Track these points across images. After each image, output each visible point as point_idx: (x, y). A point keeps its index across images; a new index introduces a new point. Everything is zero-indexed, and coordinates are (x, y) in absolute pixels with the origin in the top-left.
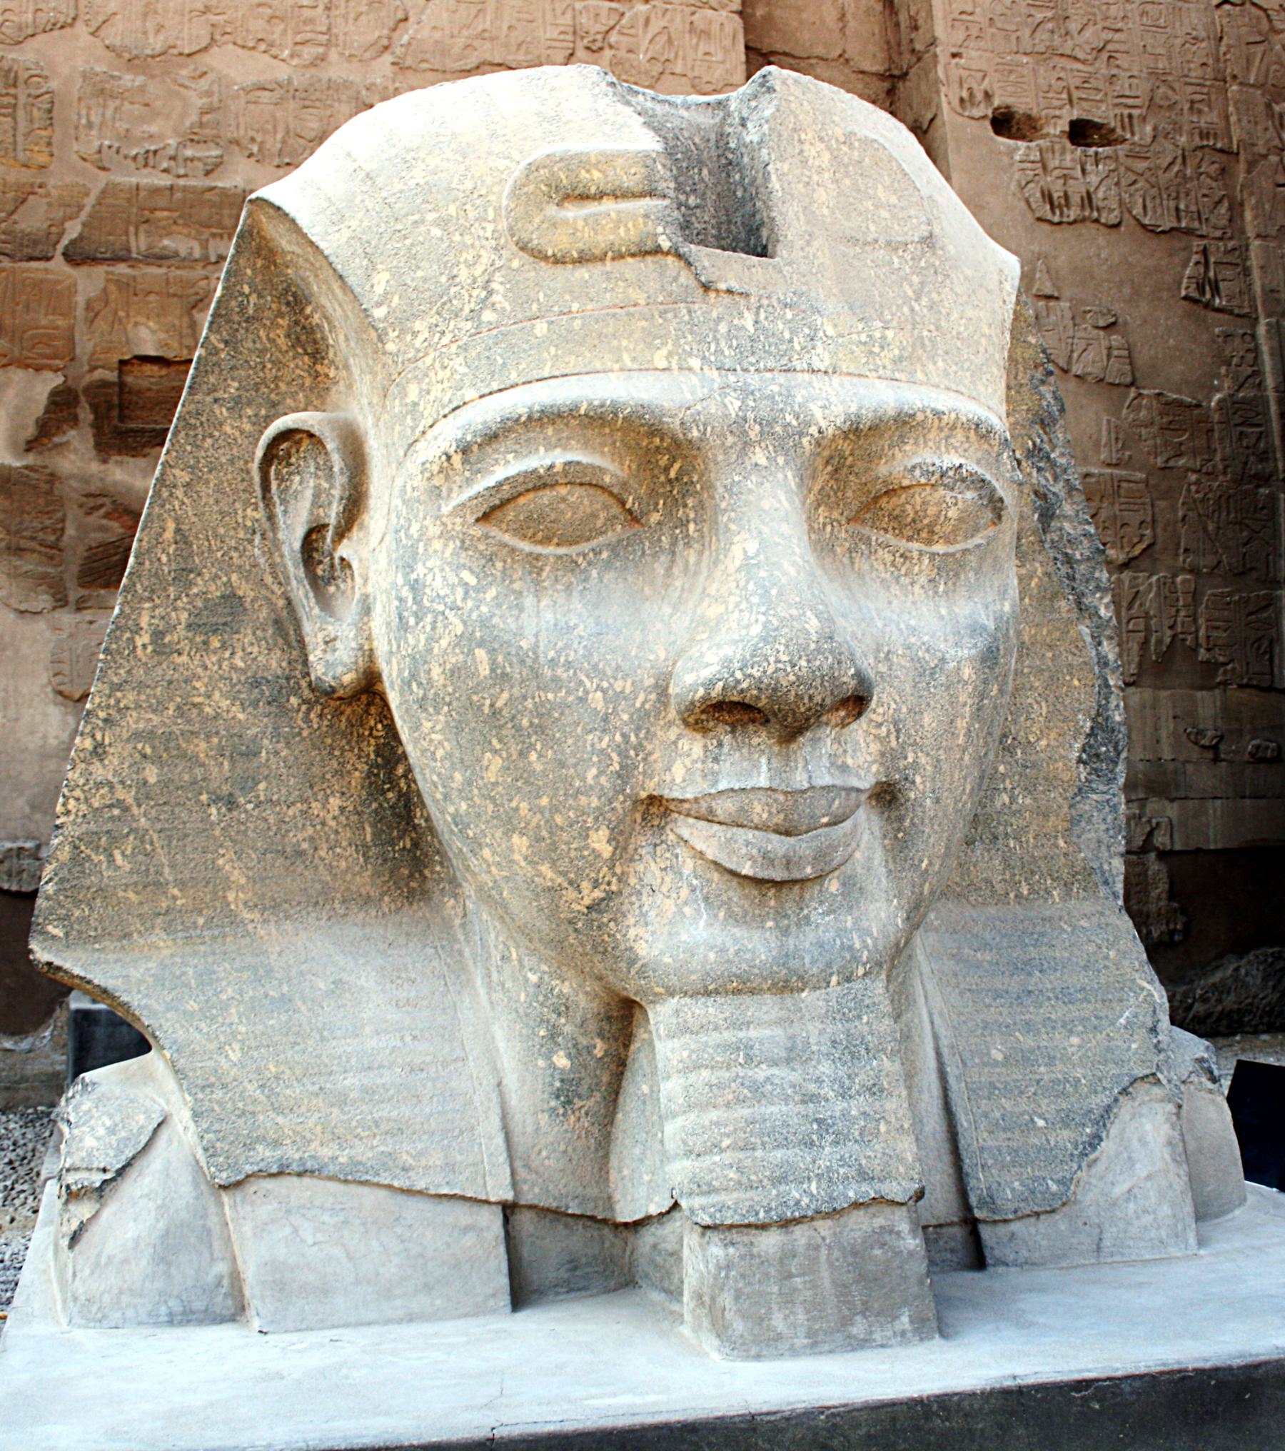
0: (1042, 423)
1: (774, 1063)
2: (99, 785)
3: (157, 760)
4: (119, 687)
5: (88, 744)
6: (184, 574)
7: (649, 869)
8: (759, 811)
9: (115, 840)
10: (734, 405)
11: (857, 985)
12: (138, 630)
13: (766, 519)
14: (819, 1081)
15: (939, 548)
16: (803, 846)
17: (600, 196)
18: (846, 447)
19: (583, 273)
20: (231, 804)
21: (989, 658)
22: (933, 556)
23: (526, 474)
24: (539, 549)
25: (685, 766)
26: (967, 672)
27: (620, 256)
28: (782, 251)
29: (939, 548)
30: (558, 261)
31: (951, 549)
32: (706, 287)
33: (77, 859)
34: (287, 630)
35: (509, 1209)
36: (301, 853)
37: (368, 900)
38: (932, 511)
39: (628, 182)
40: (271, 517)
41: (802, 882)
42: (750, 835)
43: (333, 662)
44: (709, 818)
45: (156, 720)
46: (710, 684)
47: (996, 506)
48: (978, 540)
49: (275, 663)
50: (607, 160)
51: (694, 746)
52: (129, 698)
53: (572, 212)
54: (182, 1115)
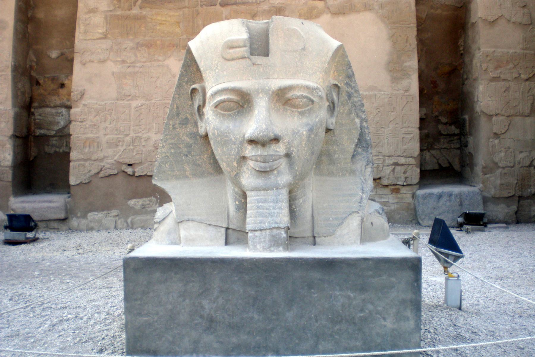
0: (348, 77)
1: (262, 202)
2: (163, 153)
3: (173, 148)
4: (166, 135)
5: (161, 145)
6: (178, 114)
7: (245, 168)
8: (259, 158)
9: (166, 163)
10: (257, 86)
11: (279, 191)
12: (170, 125)
13: (261, 108)
14: (270, 206)
15: (299, 110)
16: (267, 165)
17: (236, 47)
18: (280, 92)
19: (233, 62)
20: (187, 156)
21: (311, 130)
22: (298, 111)
23: (221, 100)
24: (225, 113)
25: (249, 151)
26: (304, 133)
27: (239, 59)
28: (270, 55)
29: (299, 110)
30: (228, 60)
31: (302, 110)
32: (254, 64)
33: (160, 166)
34: (196, 124)
35: (227, 229)
36: (199, 165)
37: (211, 174)
38: (297, 103)
39: (241, 45)
40: (193, 103)
41: (268, 171)
42: (258, 163)
43: (202, 131)
44: (252, 160)
45: (173, 141)
46: (248, 137)
47: (313, 102)
48: (309, 108)
49: (195, 130)
50: (237, 40)
51: (249, 147)
52: (168, 137)
53: (231, 51)
54: (174, 211)
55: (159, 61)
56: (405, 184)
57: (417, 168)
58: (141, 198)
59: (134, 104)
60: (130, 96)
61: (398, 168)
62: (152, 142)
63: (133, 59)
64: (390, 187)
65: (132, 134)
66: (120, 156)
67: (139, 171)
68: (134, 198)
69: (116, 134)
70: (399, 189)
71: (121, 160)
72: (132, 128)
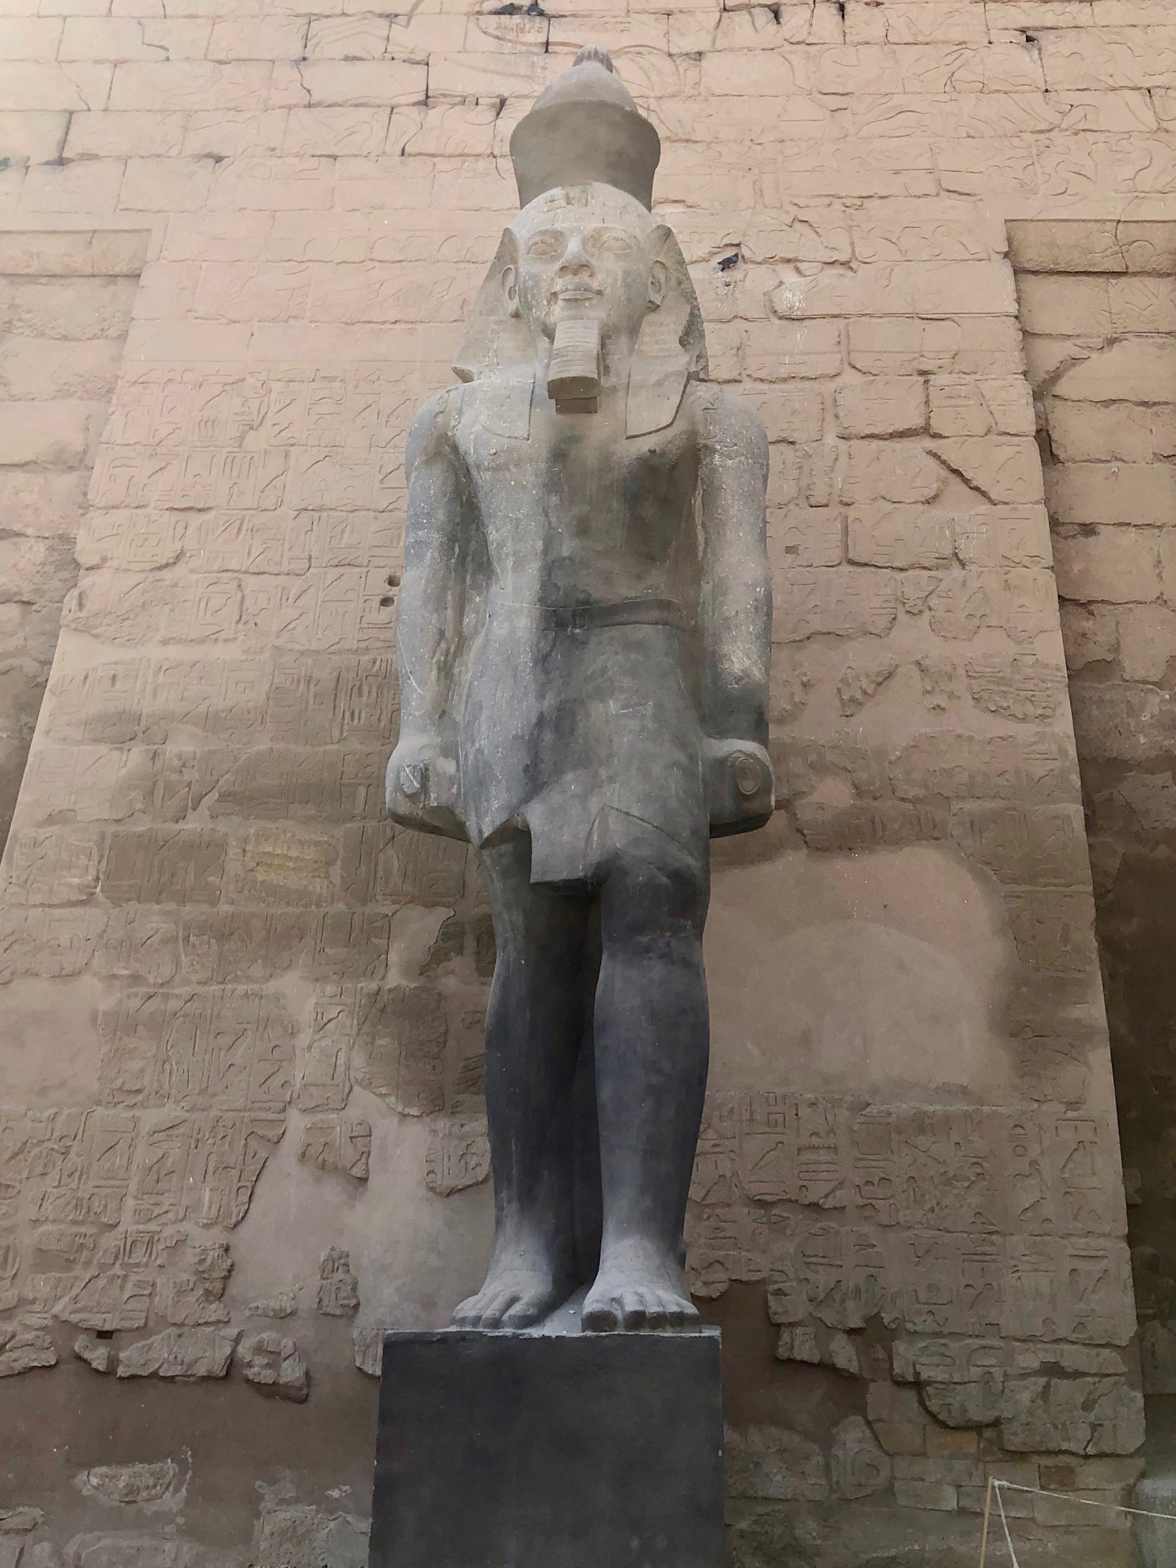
55: (249, 979)
56: (1090, 1450)
57: (1132, 1386)
58: (125, 1461)
59: (152, 1117)
60: (139, 1091)
61: (1063, 1386)
62: (190, 1256)
63: (167, 971)
64: (1035, 1458)
65: (128, 1224)
66: (75, 1299)
67: (131, 1358)
68: (101, 1462)
69: (74, 1222)
70: (1070, 1470)
71: (74, 1318)
72: (130, 1203)
